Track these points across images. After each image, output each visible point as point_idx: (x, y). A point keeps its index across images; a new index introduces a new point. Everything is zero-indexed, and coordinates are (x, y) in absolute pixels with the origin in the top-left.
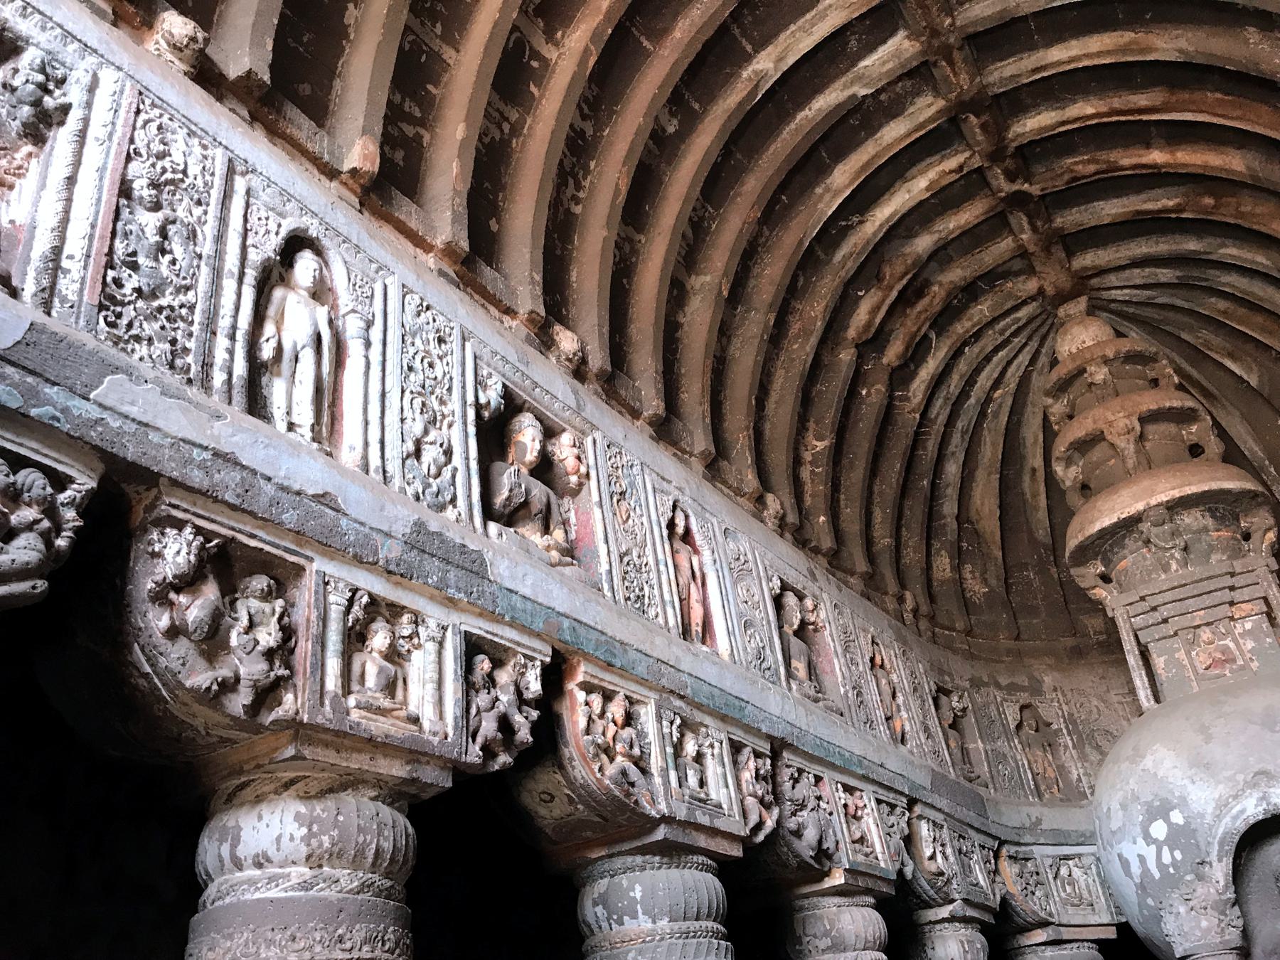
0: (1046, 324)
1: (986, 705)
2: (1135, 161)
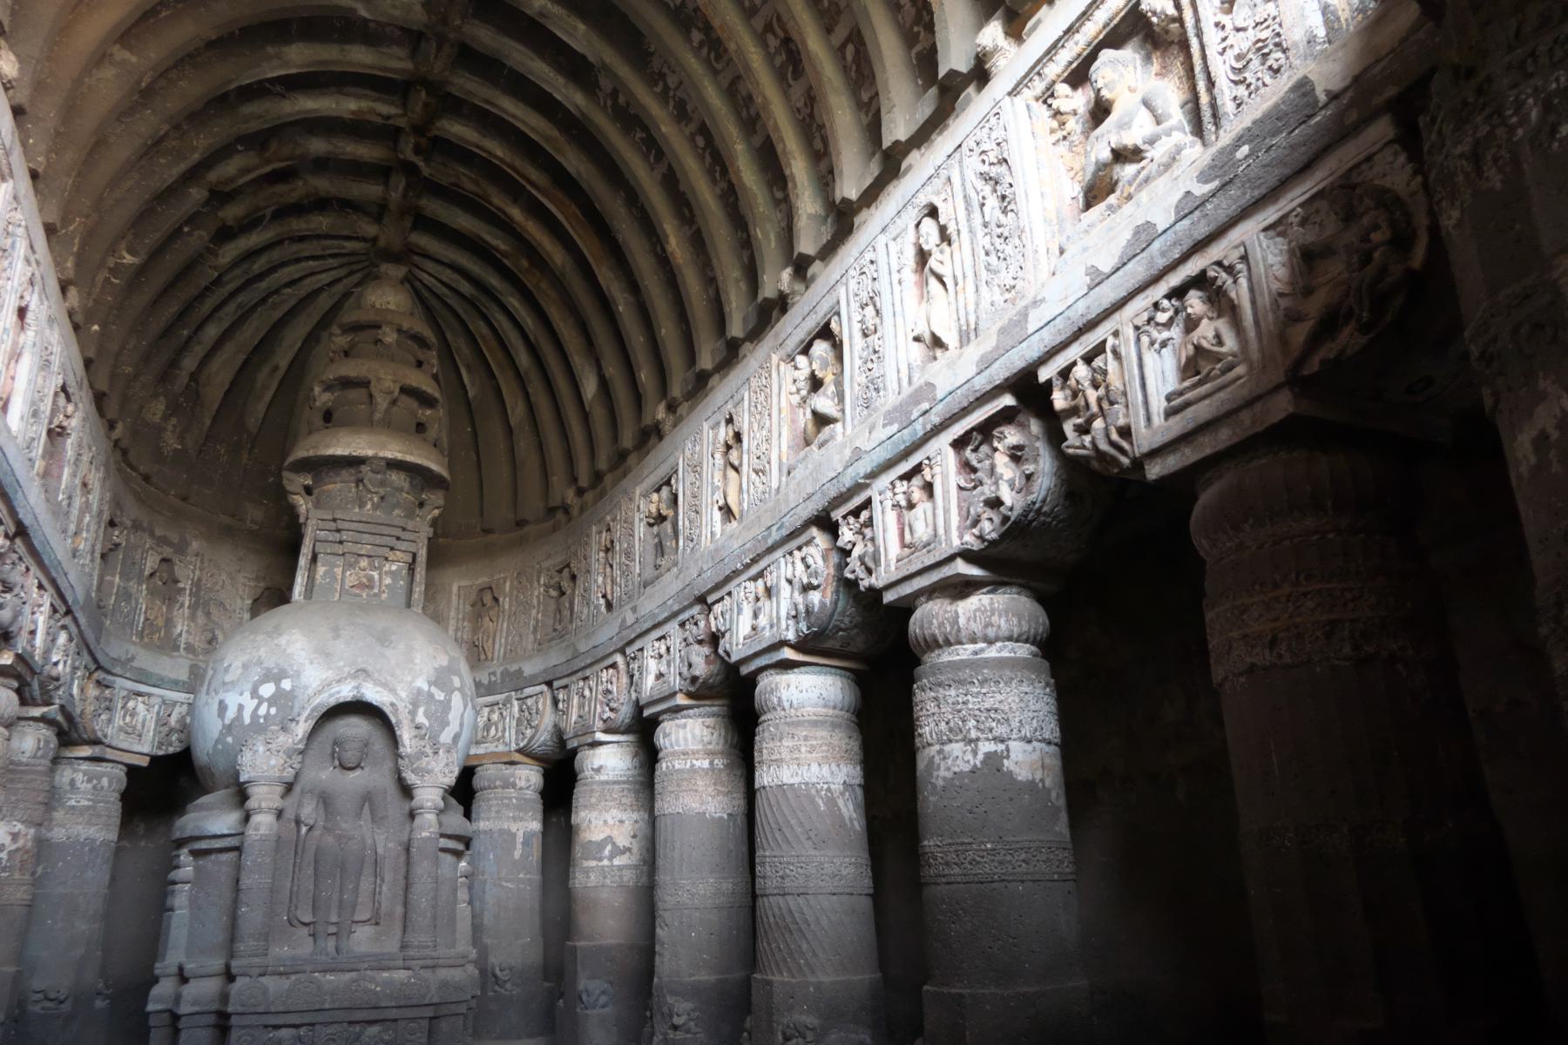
0: (366, 266)
2: (502, 205)
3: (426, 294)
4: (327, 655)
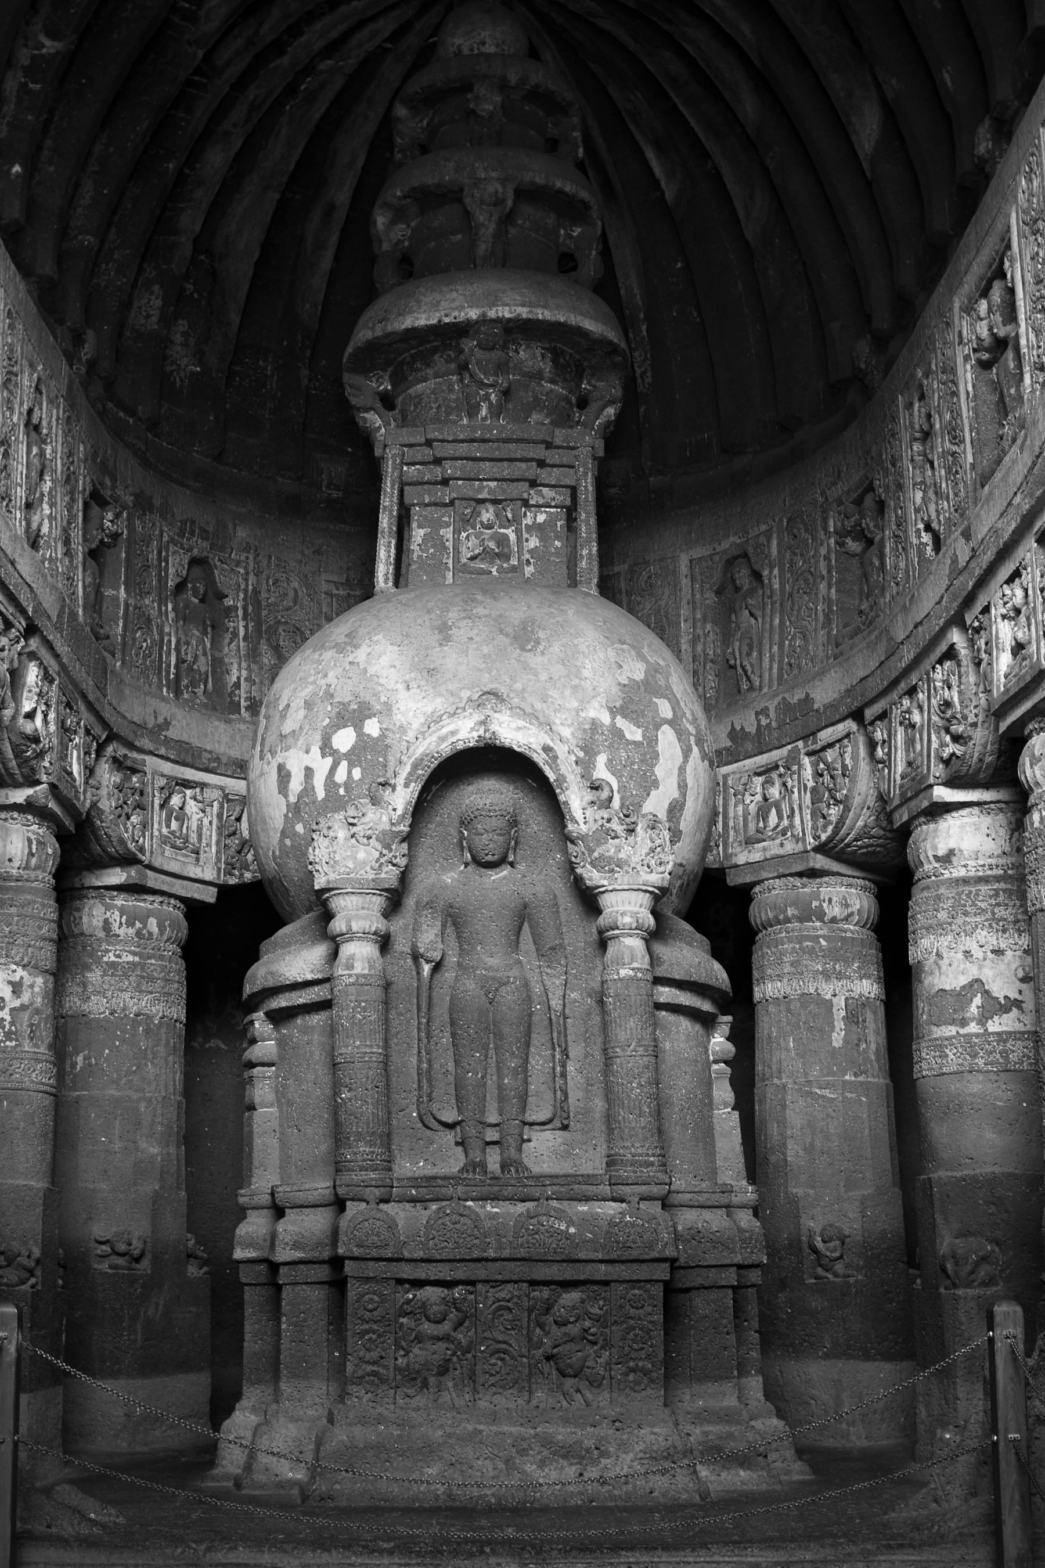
1: (147, 540)
4: (431, 672)
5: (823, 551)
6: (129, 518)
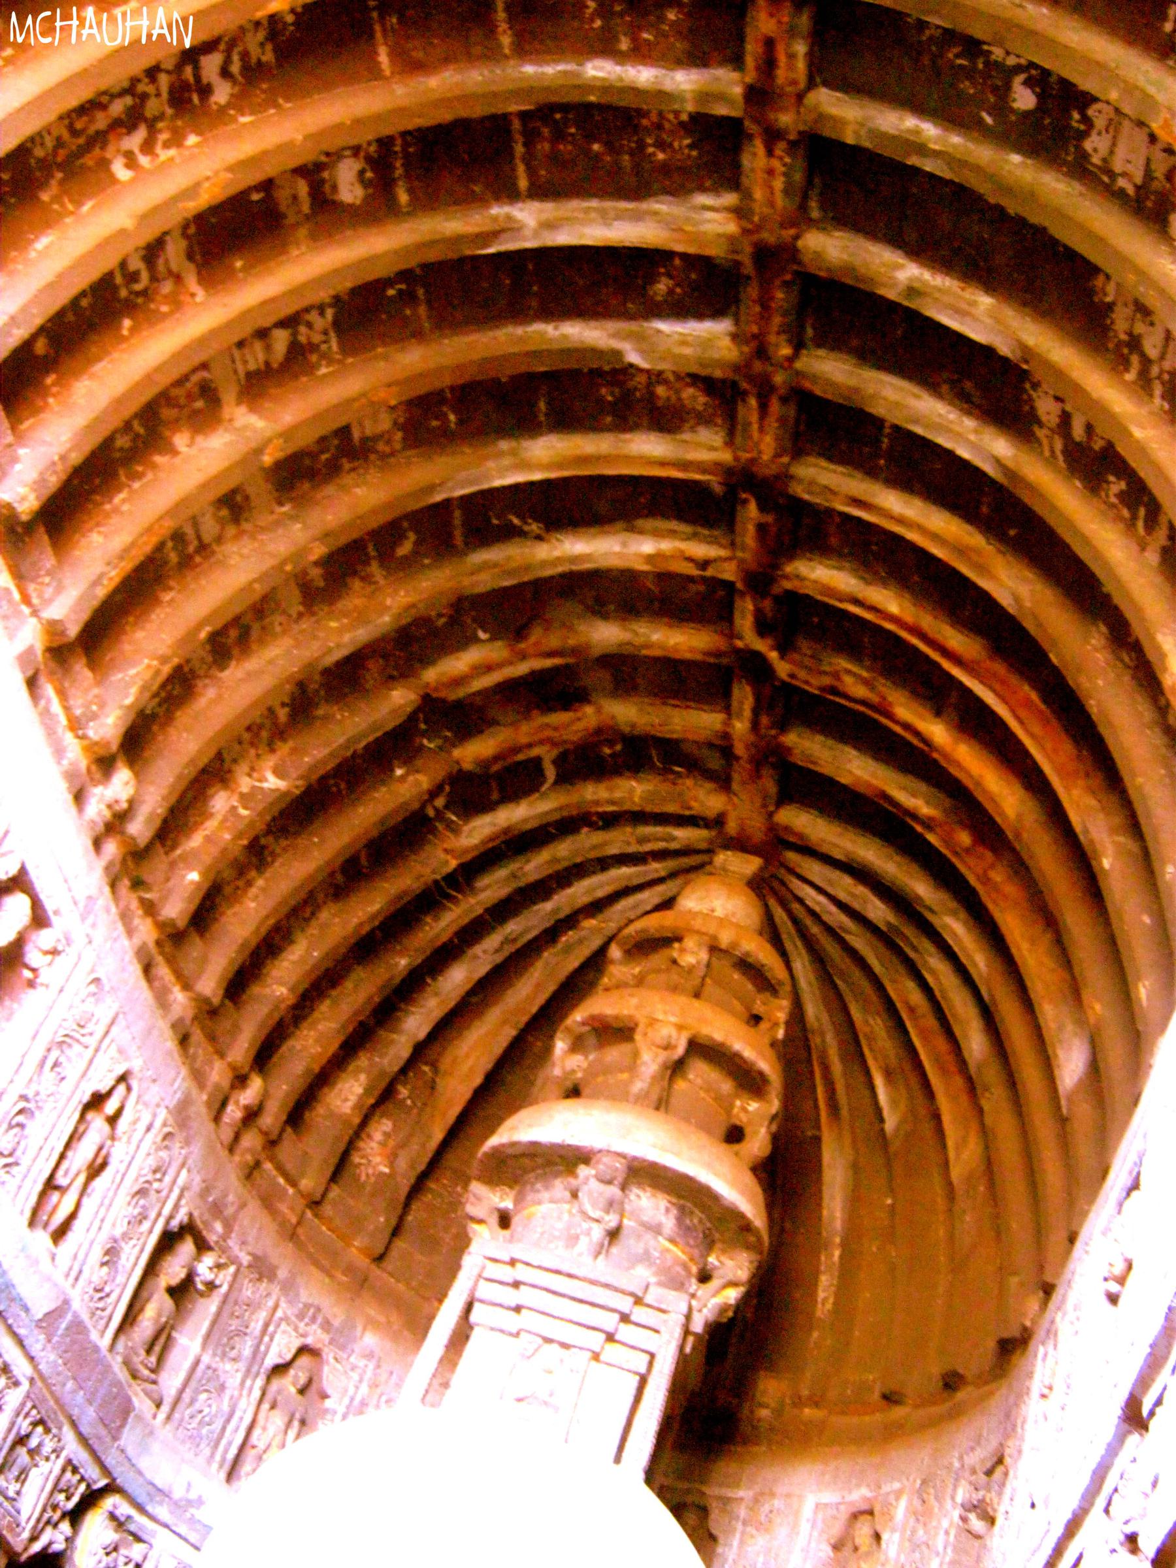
3: (815, 929)
5: (945, 1524)
6: (236, 1275)
